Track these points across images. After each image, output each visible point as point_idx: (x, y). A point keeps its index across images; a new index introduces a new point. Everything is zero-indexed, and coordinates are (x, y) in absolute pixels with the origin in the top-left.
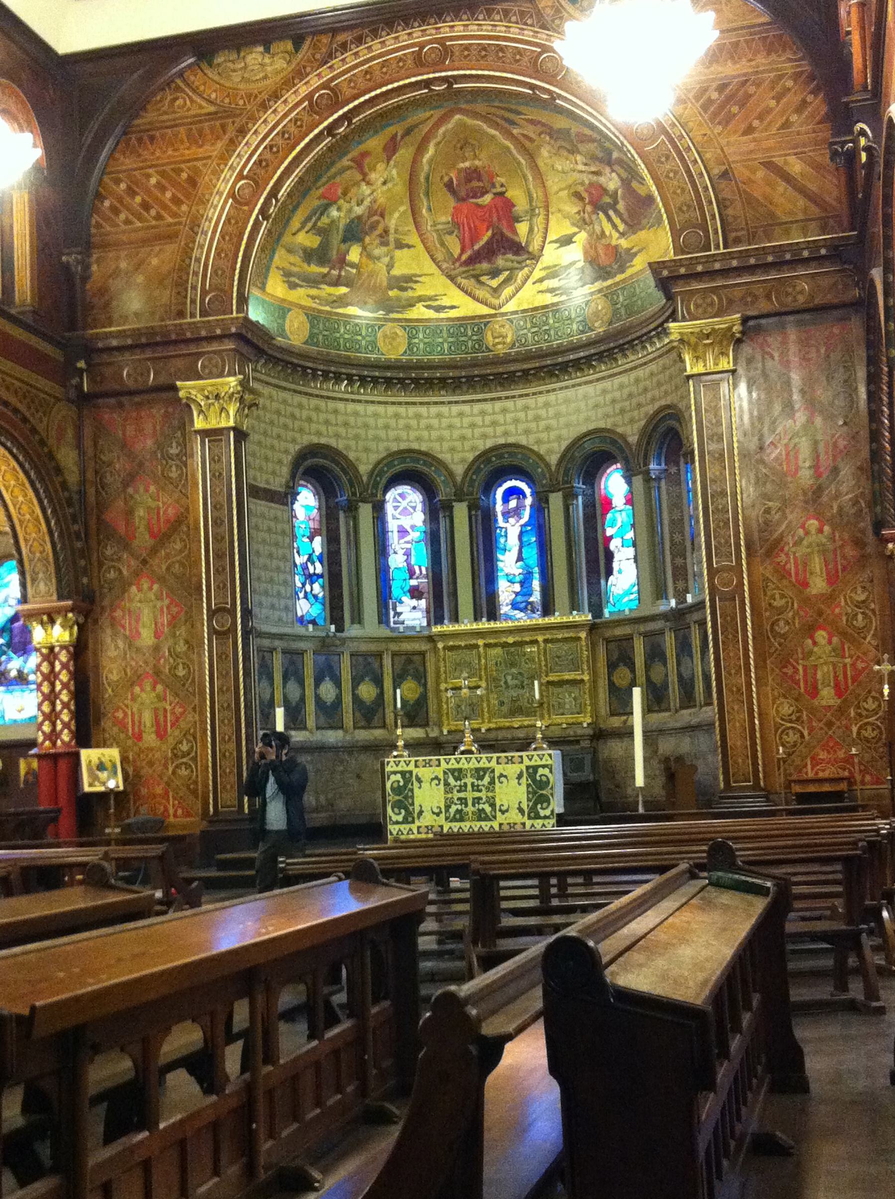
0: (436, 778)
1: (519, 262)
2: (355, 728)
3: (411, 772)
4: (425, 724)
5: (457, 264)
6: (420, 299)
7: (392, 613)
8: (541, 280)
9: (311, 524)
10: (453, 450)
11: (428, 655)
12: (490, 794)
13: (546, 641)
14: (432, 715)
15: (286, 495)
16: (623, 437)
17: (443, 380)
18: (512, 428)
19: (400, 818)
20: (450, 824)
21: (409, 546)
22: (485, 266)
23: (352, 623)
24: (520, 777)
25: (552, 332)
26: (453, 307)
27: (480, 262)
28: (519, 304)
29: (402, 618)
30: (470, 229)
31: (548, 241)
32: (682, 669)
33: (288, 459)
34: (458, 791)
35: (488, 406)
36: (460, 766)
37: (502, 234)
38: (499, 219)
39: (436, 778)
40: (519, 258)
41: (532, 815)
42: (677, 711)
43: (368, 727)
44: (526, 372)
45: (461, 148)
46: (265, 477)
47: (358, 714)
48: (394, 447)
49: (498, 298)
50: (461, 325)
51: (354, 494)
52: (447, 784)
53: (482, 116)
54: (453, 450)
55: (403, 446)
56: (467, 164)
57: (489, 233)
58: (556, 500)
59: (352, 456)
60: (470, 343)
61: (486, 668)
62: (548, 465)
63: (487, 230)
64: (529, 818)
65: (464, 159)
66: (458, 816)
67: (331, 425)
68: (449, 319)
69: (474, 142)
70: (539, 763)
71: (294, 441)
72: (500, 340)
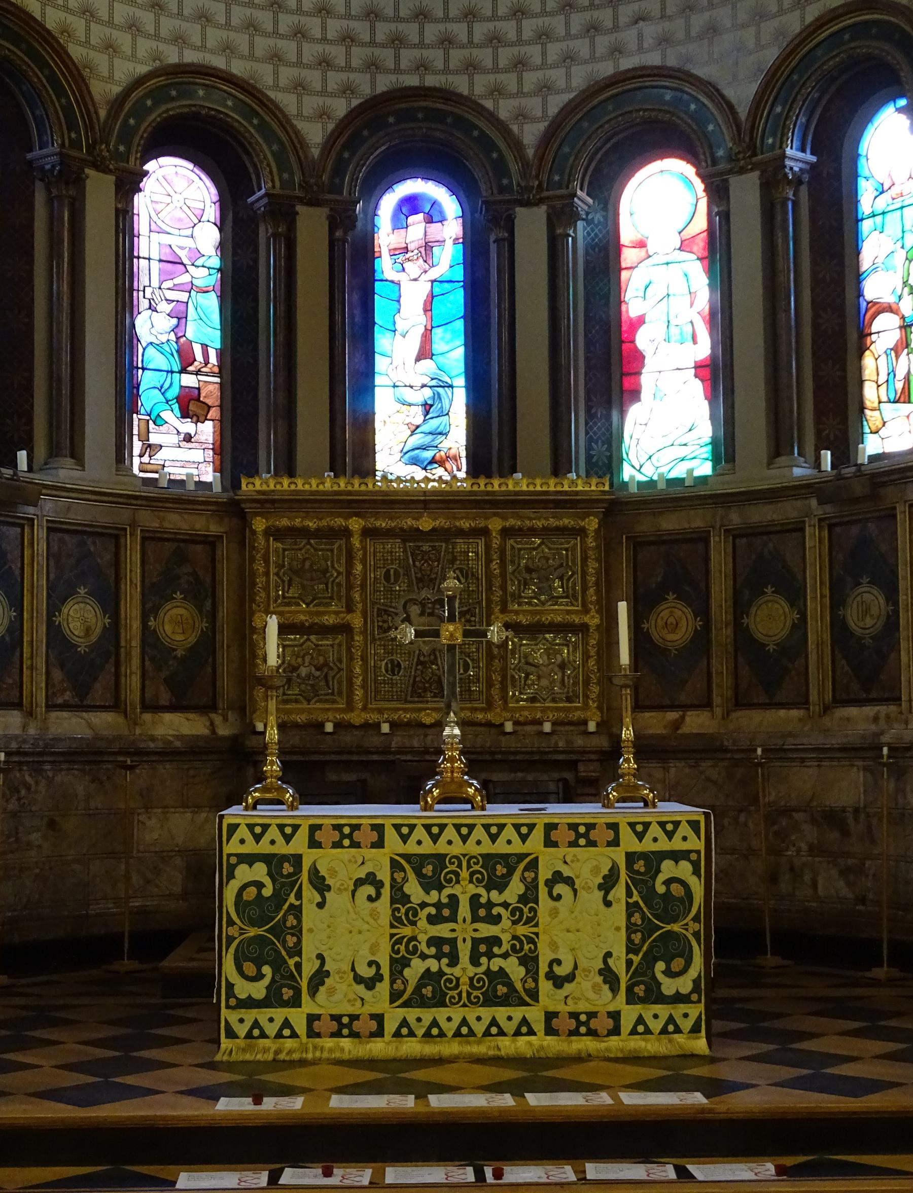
0: (371, 879)
2: (51, 706)
3: (297, 859)
4: (207, 708)
7: (137, 446)
11: (224, 550)
12: (521, 930)
13: (506, 532)
14: (226, 683)
16: (712, 90)
18: (436, 57)
19: (258, 990)
20: (402, 1012)
21: (183, 297)
23: (54, 451)
24: (608, 883)
29: (160, 456)
32: (852, 616)
34: (432, 920)
36: (441, 847)
39: (371, 879)
41: (640, 990)
42: (826, 709)
43: (79, 706)
47: (57, 674)
51: (75, 144)
52: (399, 897)
54: (300, 87)
55: (191, 57)
61: (363, 586)
62: (516, 145)
64: (631, 999)
66: (428, 991)
70: (664, 845)
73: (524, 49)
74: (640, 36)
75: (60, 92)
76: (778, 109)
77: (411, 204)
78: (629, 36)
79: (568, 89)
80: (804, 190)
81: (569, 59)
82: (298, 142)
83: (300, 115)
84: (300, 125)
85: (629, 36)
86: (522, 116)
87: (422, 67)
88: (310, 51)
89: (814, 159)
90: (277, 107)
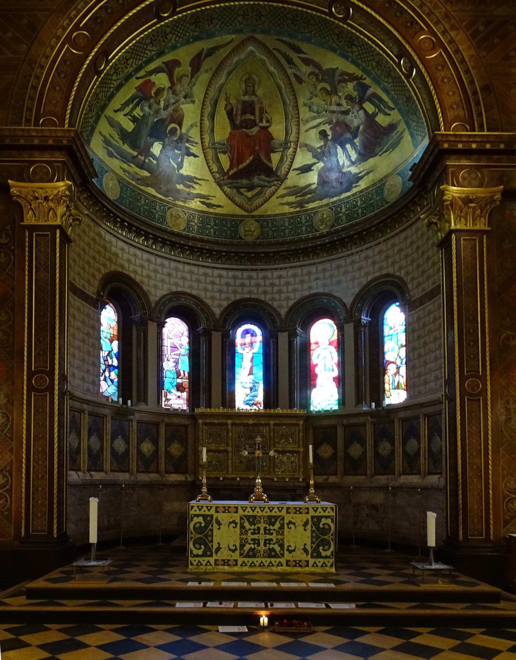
1: (268, 182)
5: (226, 178)
6: (199, 196)
8: (283, 196)
9: (111, 331)
10: (213, 298)
15: (97, 301)
17: (210, 251)
18: (255, 290)
22: (245, 181)
25: (287, 232)
26: (219, 206)
27: (241, 178)
28: (265, 211)
30: (238, 152)
31: (292, 169)
33: (99, 276)
35: (238, 274)
37: (260, 160)
38: (260, 148)
40: (270, 179)
44: (267, 254)
45: (245, 82)
46: (82, 281)
48: (174, 289)
49: (251, 205)
50: (224, 220)
53: (269, 51)
55: (180, 289)
56: (247, 98)
57: (251, 158)
58: (283, 338)
59: (145, 288)
60: (229, 232)
62: (279, 314)
63: (250, 155)
65: (246, 93)
67: (132, 264)
68: (216, 214)
69: (256, 79)
71: (104, 265)
72: (250, 233)
73: (281, 287)
74: (317, 284)
75: (140, 299)
76: (359, 305)
77: (247, 332)
78: (314, 284)
79: (295, 298)
80: (367, 328)
81: (295, 290)
82: (212, 313)
83: (213, 306)
84: (213, 309)
85: (314, 284)
86: (281, 306)
87: (250, 292)
88: (216, 288)
89: (370, 319)
90: (206, 303)
